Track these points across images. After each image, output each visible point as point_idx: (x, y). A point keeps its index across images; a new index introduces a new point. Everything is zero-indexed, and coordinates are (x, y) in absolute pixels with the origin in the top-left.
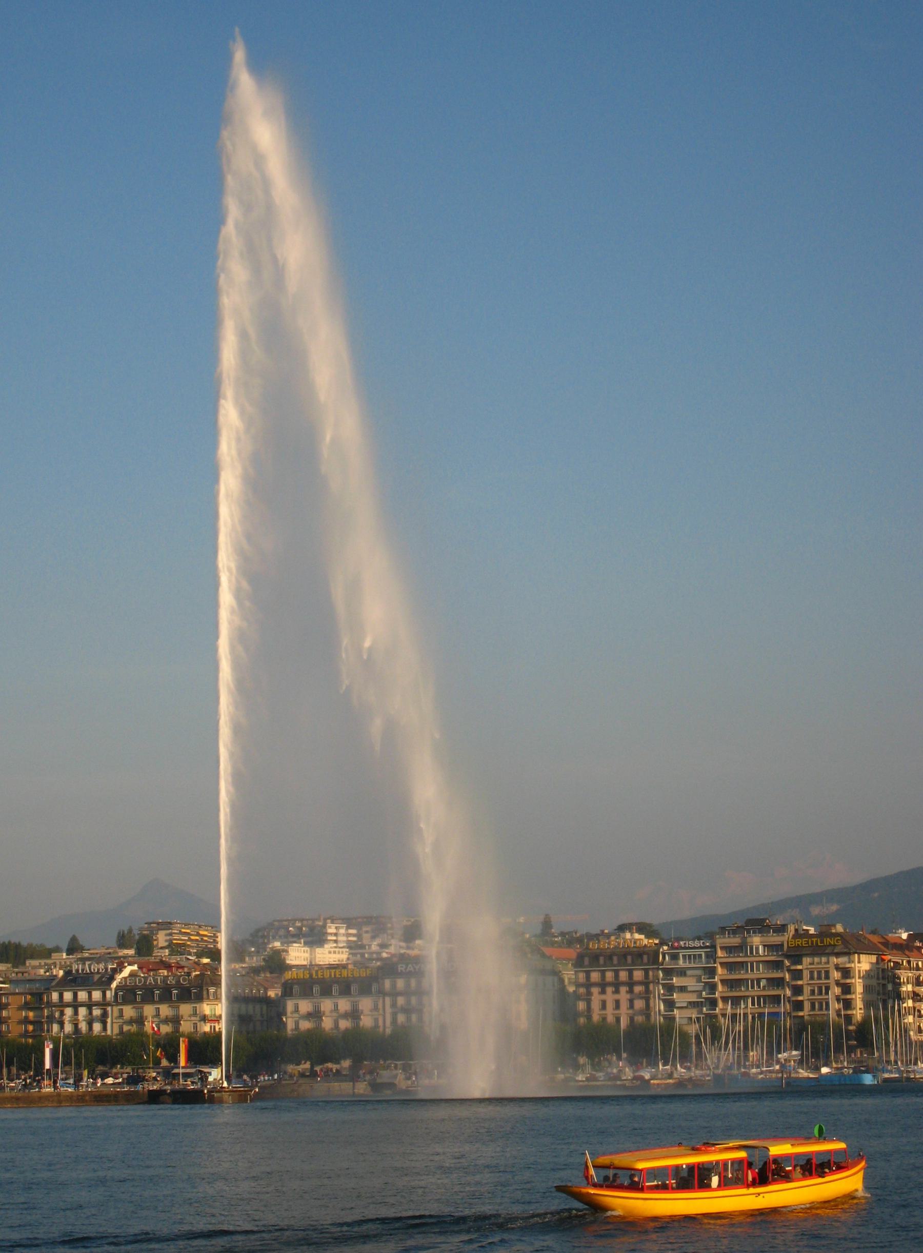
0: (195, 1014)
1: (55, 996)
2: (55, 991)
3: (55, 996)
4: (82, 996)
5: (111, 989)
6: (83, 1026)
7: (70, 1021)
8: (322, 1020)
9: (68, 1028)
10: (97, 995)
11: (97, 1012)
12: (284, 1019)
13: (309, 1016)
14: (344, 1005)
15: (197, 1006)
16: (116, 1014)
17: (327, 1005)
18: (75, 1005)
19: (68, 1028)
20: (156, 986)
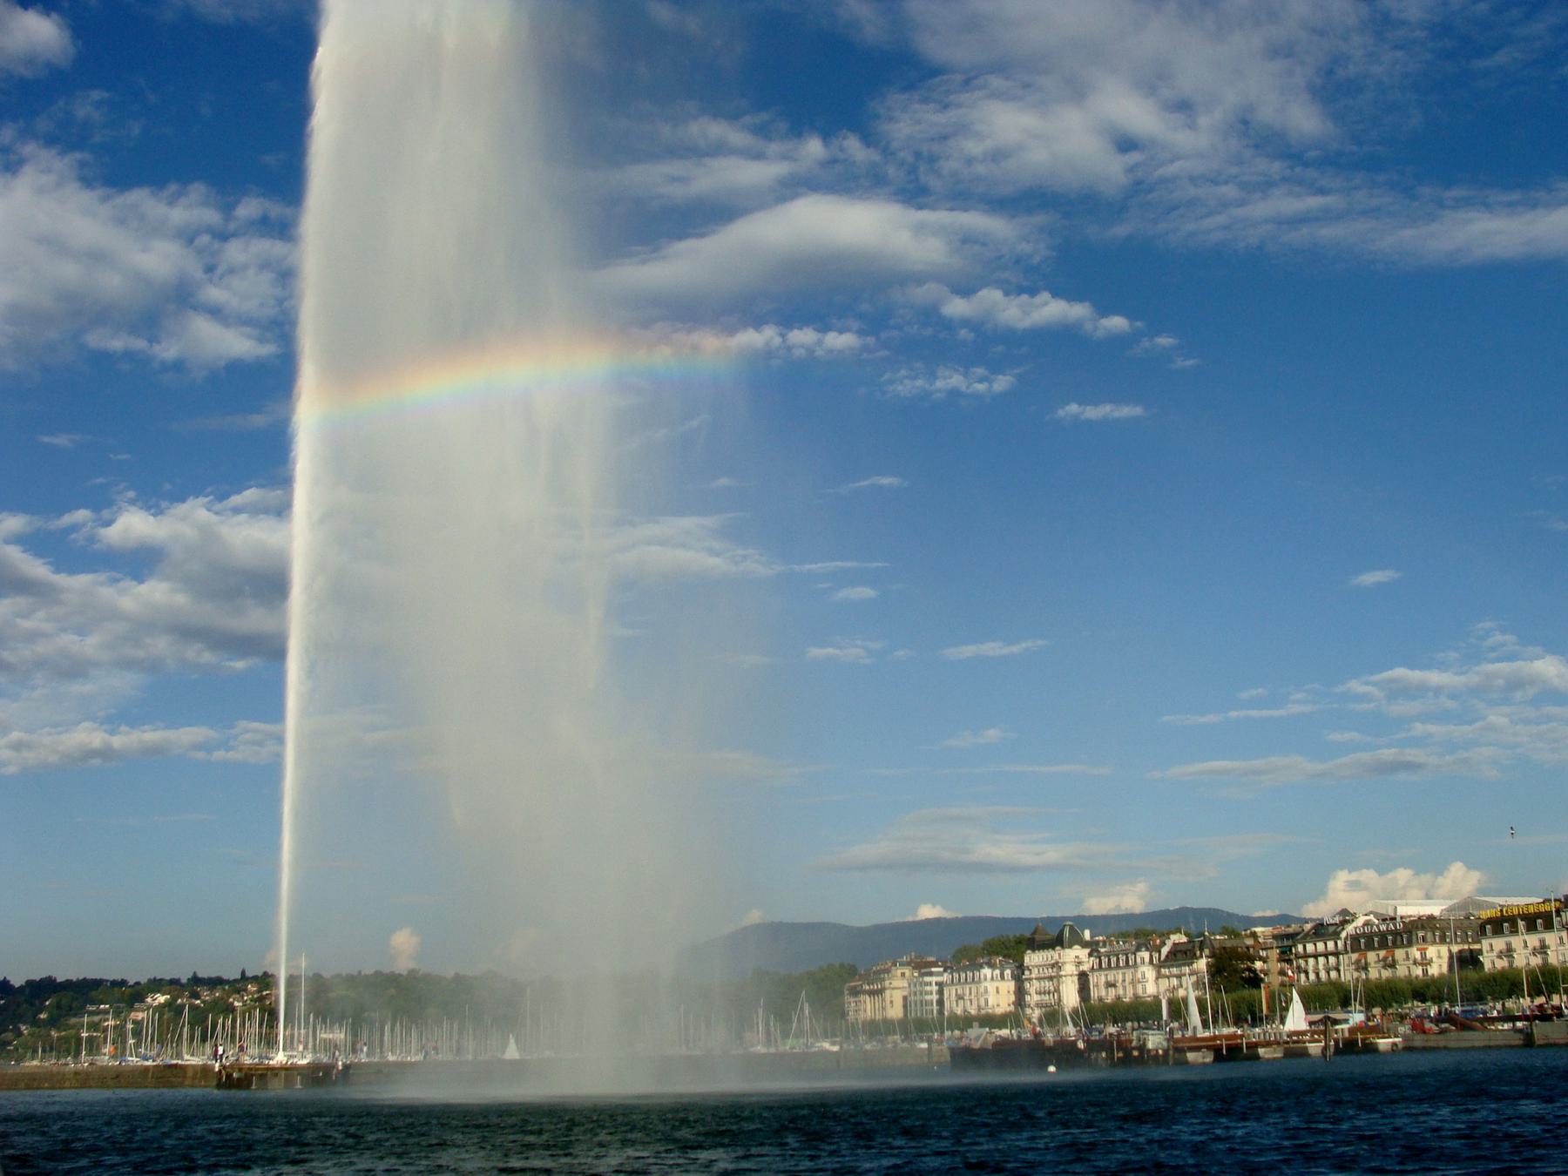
0: (1408, 958)
1: (1300, 948)
2: (1300, 943)
3: (1300, 948)
4: (1321, 946)
5: (1340, 939)
6: (1323, 975)
7: (1314, 972)
8: (1514, 957)
9: (1312, 976)
10: (1331, 945)
11: (1332, 960)
12: (1481, 959)
13: (1535, 952)
14: (1533, 940)
15: (1409, 950)
16: (1347, 961)
17: (1516, 941)
18: (1316, 956)
19: (1312, 976)
20: (1376, 934)
